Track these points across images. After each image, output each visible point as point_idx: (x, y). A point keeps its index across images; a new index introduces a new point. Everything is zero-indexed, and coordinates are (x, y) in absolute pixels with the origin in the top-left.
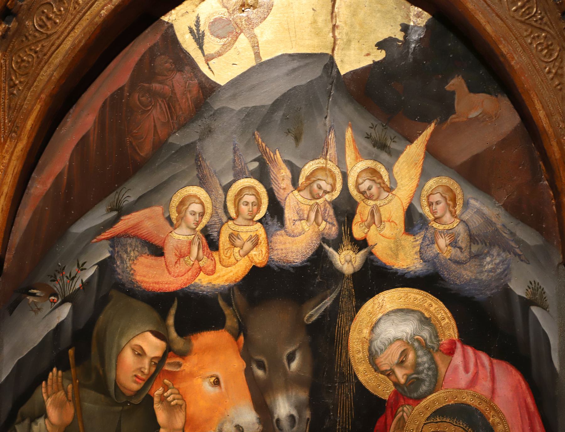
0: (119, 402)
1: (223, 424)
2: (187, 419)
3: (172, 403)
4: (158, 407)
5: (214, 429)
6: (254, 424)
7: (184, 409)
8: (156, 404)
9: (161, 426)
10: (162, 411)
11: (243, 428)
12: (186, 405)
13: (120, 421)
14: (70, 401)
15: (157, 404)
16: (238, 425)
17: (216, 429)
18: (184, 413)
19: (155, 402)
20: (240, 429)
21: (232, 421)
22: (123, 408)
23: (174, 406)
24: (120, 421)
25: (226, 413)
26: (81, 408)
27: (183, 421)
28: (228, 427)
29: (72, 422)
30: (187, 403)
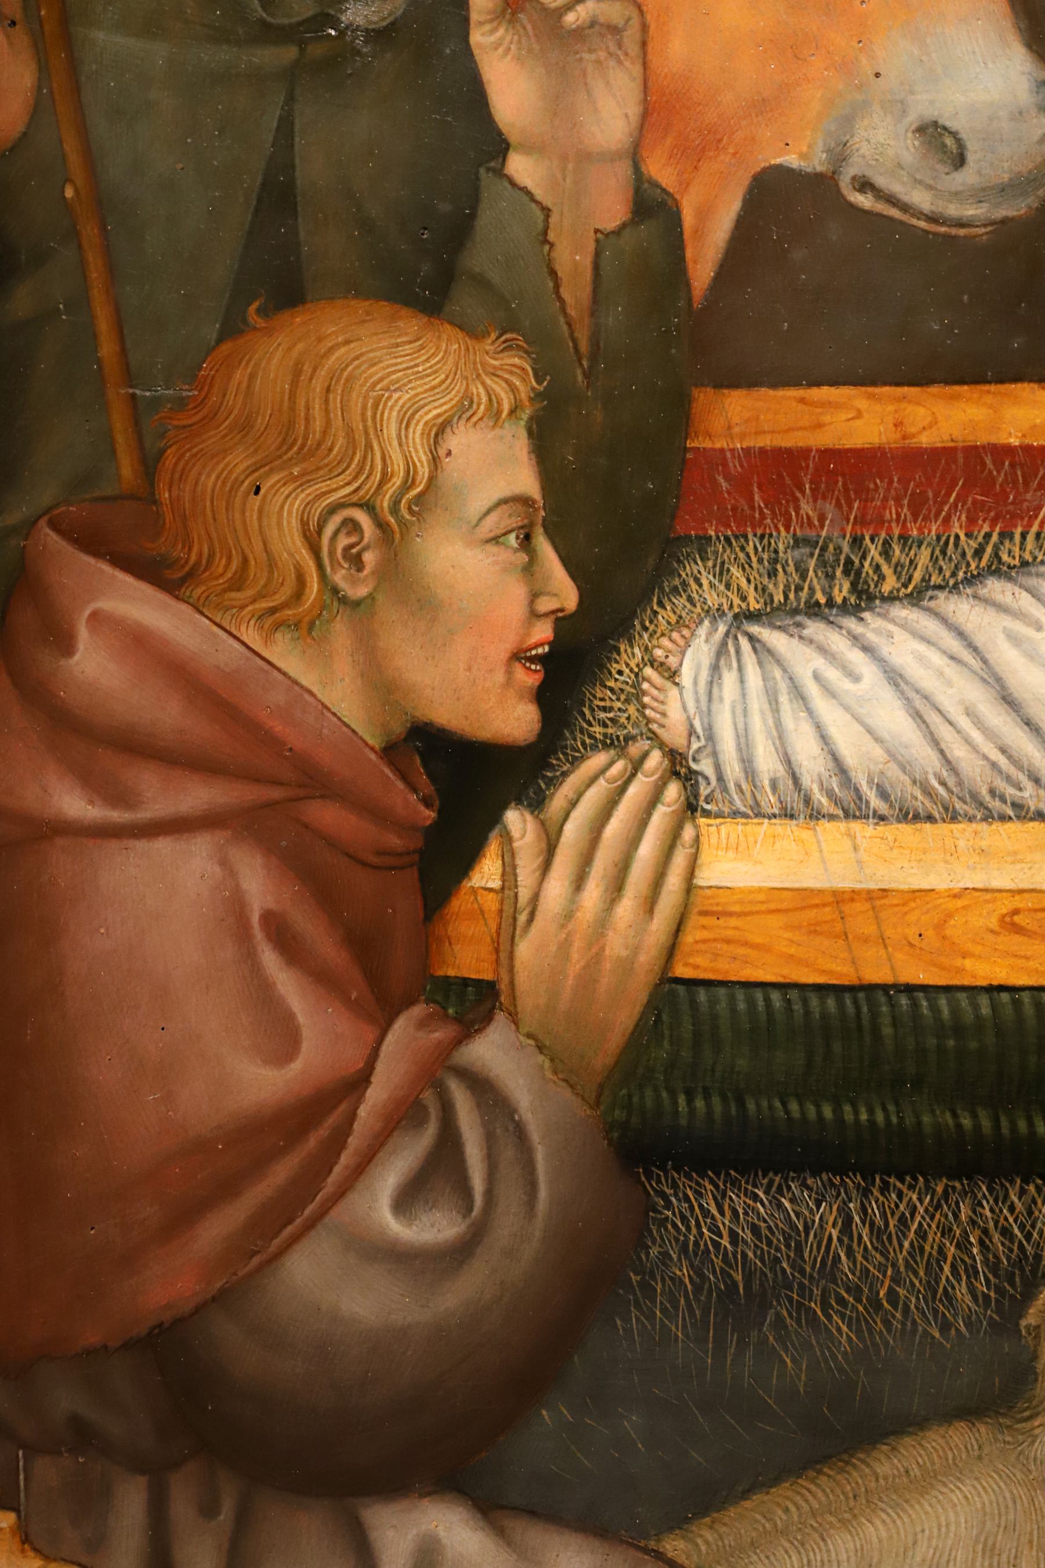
0: (286, 21)
1: (848, 121)
2: (652, 98)
3: (570, 18)
4: (492, 39)
5: (805, 149)
6: (1018, 116)
7: (634, 49)
8: (481, 24)
9: (513, 137)
10: (518, 59)
11: (963, 135)
12: (644, 27)
13: (286, 128)
14: (13, 23)
15: (487, 27)
16: (935, 124)
17: (810, 146)
18: (637, 70)
19: (474, 17)
20: (944, 146)
21: (902, 102)
22: (302, 51)
23: (579, 34)
24: (286, 128)
25: (866, 67)
26: (73, 67)
27: (634, 110)
28: (880, 135)
29: (25, 134)
30: (648, 17)
